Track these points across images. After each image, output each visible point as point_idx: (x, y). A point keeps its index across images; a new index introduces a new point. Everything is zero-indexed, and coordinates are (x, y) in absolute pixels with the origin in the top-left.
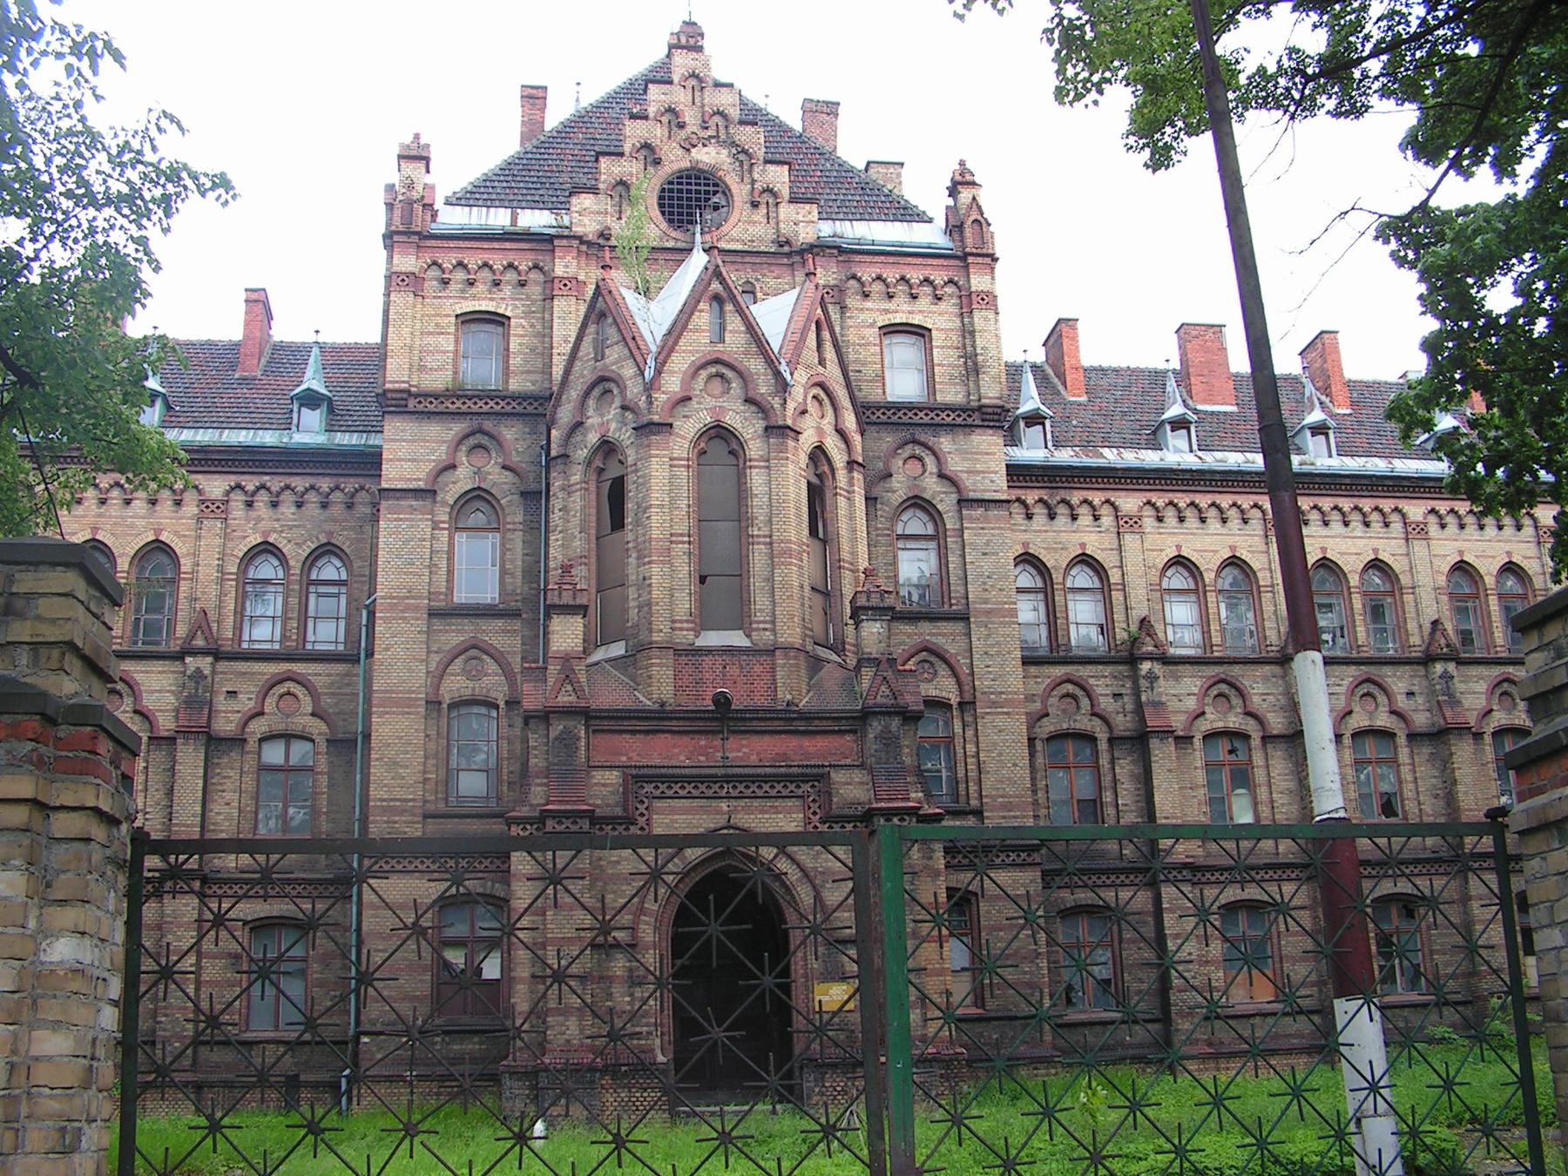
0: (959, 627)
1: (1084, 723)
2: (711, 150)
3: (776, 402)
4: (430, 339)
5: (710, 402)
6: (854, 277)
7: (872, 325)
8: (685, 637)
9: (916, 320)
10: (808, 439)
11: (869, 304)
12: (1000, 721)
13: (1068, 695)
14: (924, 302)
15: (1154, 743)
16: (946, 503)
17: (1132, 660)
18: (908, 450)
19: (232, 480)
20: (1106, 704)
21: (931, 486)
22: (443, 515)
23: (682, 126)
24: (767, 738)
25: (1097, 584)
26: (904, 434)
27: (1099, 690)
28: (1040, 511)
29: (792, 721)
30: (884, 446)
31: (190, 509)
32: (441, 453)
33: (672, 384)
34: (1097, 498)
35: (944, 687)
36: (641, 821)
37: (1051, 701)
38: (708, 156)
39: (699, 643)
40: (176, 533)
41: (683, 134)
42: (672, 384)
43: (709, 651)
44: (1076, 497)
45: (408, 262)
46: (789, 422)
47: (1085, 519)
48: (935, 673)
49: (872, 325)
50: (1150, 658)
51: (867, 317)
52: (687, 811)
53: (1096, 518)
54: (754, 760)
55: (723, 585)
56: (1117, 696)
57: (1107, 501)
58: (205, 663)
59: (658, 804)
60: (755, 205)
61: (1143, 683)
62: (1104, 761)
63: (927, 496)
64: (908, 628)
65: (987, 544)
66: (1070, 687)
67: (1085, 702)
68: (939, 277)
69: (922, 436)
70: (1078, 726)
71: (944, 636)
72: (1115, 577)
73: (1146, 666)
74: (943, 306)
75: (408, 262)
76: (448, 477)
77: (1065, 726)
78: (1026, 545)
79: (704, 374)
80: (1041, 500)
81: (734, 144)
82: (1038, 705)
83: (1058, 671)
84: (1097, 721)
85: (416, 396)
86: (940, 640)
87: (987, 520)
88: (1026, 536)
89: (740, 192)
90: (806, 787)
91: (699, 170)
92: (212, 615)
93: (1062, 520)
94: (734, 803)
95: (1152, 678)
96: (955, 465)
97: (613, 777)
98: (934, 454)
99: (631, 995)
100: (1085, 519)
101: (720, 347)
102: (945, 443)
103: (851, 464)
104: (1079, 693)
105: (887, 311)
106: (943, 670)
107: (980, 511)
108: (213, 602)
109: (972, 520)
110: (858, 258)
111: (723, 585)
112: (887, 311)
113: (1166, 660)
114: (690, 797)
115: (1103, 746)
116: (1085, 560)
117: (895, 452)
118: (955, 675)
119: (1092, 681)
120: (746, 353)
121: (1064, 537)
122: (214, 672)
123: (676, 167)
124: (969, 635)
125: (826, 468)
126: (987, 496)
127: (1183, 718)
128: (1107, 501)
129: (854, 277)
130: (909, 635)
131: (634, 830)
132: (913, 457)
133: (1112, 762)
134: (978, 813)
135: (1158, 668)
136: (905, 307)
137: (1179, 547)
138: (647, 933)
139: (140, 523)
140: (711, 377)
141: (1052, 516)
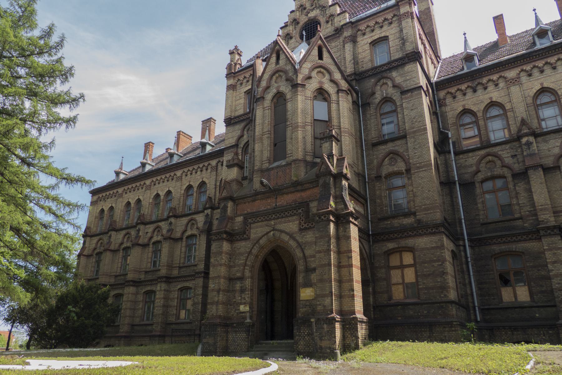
0: (403, 141)
1: (498, 171)
2: (314, 12)
3: (294, 77)
4: (238, 102)
5: (276, 85)
6: (359, 30)
7: (367, 44)
8: (266, 166)
9: (383, 35)
10: (313, 85)
11: (365, 37)
12: (421, 174)
13: (490, 161)
14: (385, 28)
15: (530, 172)
16: (396, 96)
17: (518, 138)
18: (382, 81)
19: (217, 160)
20: (509, 161)
21: (391, 91)
22: (240, 151)
23: (305, 9)
24: (290, 195)
25: (502, 112)
26: (379, 76)
27: (504, 156)
28: (469, 92)
29: (297, 185)
30: (371, 84)
31: (209, 171)
32: (238, 133)
33: (264, 84)
34: (495, 77)
35: (401, 166)
36: (247, 232)
37: (482, 165)
38: (312, 15)
39: (271, 166)
40: (206, 178)
41: (305, 11)
42: (264, 84)
43: (273, 168)
44: (484, 80)
45: (232, 82)
46: (299, 82)
47: (491, 87)
48: (396, 162)
49: (367, 44)
50: (526, 135)
51: (365, 41)
52: (261, 227)
53: (496, 85)
54: (285, 204)
55: (279, 145)
56: (513, 156)
57: (501, 77)
58: (209, 211)
59: (253, 226)
60: (327, 22)
61: (525, 147)
62: (511, 186)
63: (389, 96)
64: (383, 147)
65: (413, 105)
66: (490, 158)
67: (499, 163)
68: (389, 16)
69: (385, 74)
70: (495, 173)
71: (397, 146)
72: (508, 106)
73: (524, 140)
74: (393, 25)
75: (232, 82)
76: (242, 139)
77: (489, 174)
78: (464, 106)
79: (274, 77)
80: (468, 87)
81: (320, 6)
82: (474, 168)
83: (483, 152)
84: (505, 169)
85: (234, 118)
86: (397, 148)
87: (412, 96)
88: (464, 103)
89: (322, 20)
90: (300, 211)
91: (312, 20)
92: (213, 198)
93: (480, 91)
94: (276, 221)
95: (529, 144)
96: (399, 80)
97: (240, 219)
98: (391, 79)
99: (241, 296)
100: (491, 87)
101: (278, 66)
102: (394, 74)
103: (339, 91)
104: (495, 159)
105: (372, 37)
106: (399, 160)
107: (409, 94)
108: (213, 193)
109: (406, 98)
110: (361, 22)
111: (279, 145)
112: (372, 37)
113: (536, 135)
114: (262, 221)
115: (510, 179)
116: (492, 104)
117: (376, 84)
118: (404, 160)
119: (500, 153)
120: (286, 64)
121: (481, 97)
122: (212, 213)
123: (303, 22)
124: (407, 143)
125: (326, 96)
126: (412, 87)
127: (552, 159)
128: (501, 77)
129: (359, 30)
130: (384, 149)
131: (245, 236)
132: (384, 84)
133: (515, 186)
134: (414, 214)
135: (531, 139)
136: (379, 32)
137: (542, 84)
138: (247, 274)
139: (199, 177)
140: (277, 78)
141: (475, 91)
